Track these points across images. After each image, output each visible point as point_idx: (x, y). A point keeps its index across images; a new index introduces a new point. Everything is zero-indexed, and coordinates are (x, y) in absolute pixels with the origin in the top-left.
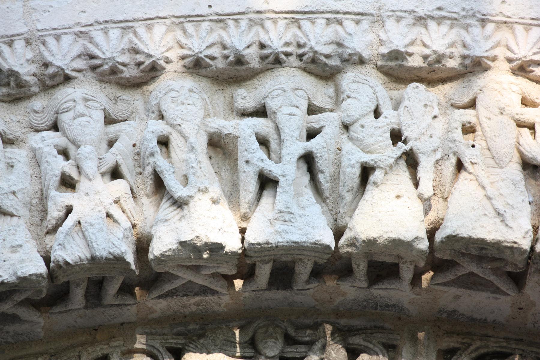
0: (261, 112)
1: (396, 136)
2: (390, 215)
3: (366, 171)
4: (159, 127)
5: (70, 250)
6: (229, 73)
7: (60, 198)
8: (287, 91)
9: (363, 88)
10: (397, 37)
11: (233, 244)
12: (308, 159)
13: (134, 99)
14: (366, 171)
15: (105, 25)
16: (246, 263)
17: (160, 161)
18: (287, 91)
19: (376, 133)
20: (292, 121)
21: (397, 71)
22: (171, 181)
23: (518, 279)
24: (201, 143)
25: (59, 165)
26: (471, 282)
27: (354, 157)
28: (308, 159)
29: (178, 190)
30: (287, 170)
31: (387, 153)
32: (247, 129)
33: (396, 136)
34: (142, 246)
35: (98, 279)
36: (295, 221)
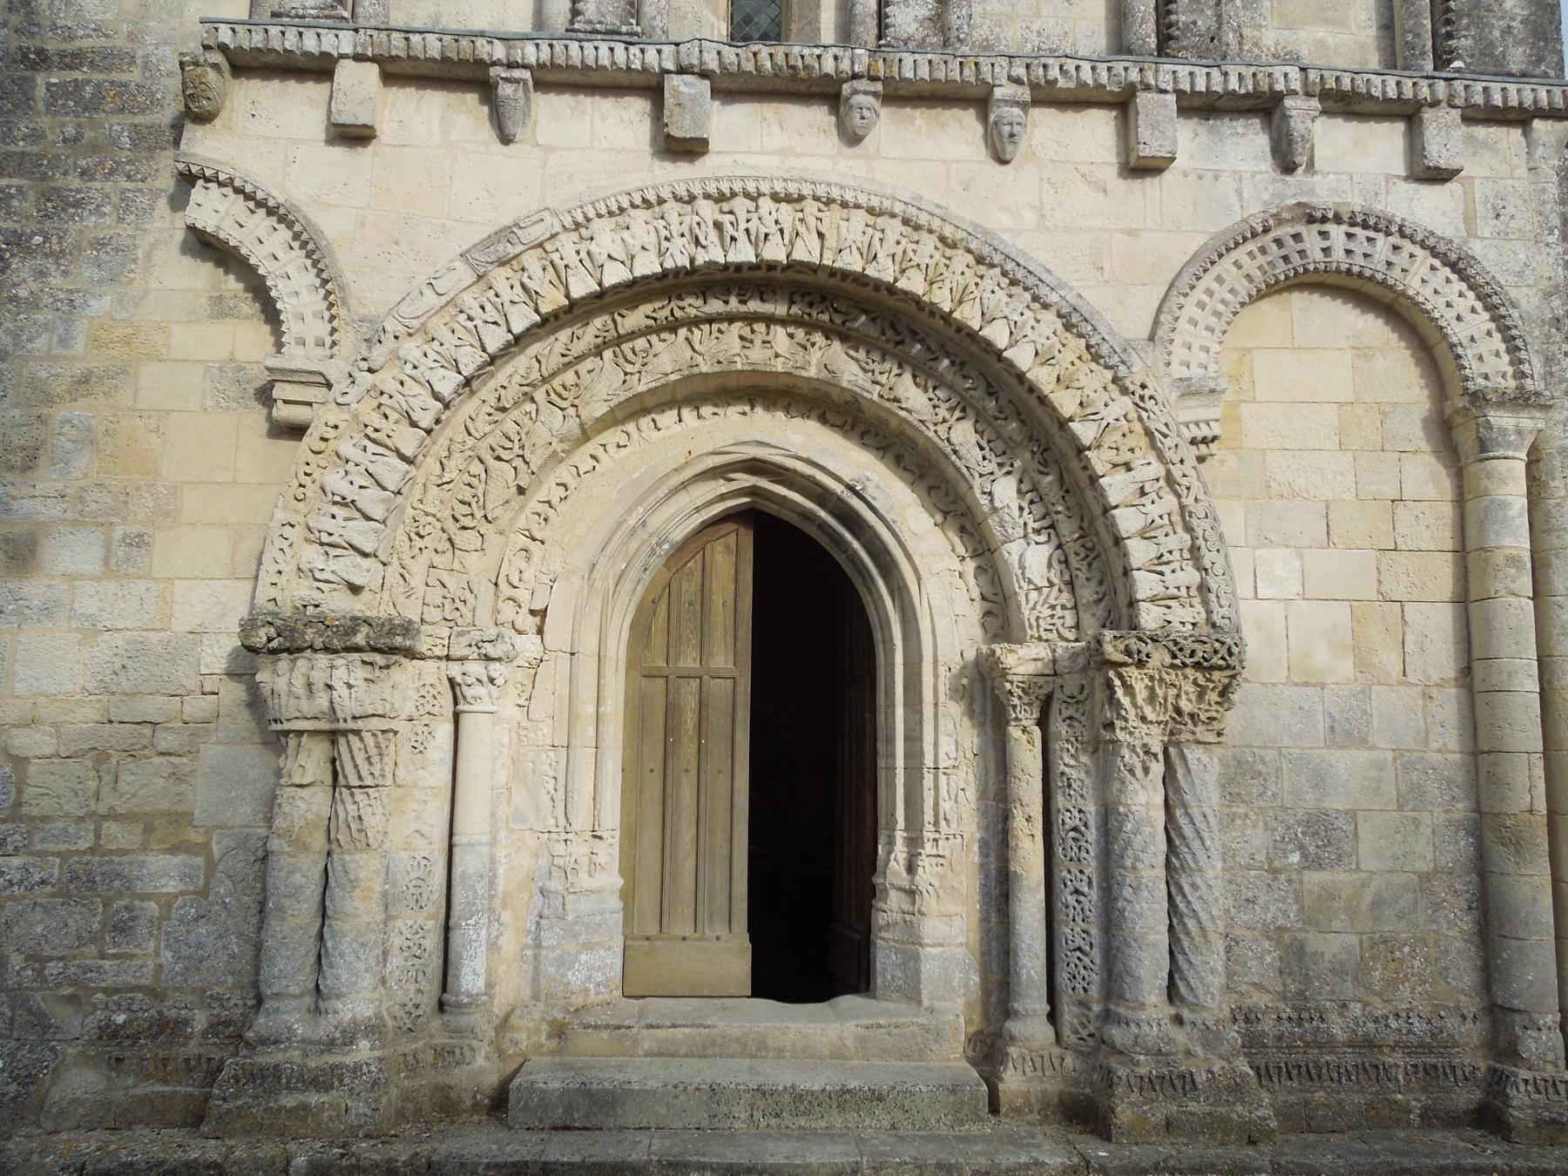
0: (731, 212)
1: (777, 222)
2: (775, 252)
3: (766, 235)
4: (696, 219)
5: (669, 264)
6: (721, 198)
7: (665, 244)
8: (740, 205)
9: (766, 204)
10: (779, 187)
11: (722, 261)
12: (747, 230)
13: (688, 207)
14: (766, 235)
15: (678, 181)
16: (726, 266)
17: (697, 231)
18: (740, 205)
19: (770, 221)
20: (742, 217)
21: (776, 198)
22: (702, 239)
23: (815, 271)
24: (710, 224)
25: (664, 233)
26: (799, 272)
27: (763, 230)
28: (747, 230)
29: (704, 243)
30: (741, 235)
31: (773, 229)
32: (726, 219)
33: (777, 222)
34: (692, 261)
35: (677, 271)
36: (743, 253)
